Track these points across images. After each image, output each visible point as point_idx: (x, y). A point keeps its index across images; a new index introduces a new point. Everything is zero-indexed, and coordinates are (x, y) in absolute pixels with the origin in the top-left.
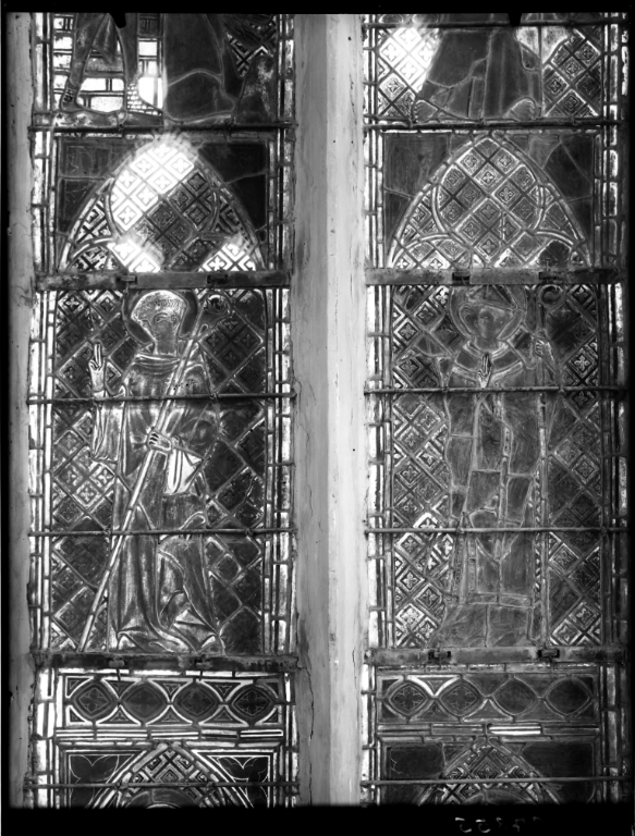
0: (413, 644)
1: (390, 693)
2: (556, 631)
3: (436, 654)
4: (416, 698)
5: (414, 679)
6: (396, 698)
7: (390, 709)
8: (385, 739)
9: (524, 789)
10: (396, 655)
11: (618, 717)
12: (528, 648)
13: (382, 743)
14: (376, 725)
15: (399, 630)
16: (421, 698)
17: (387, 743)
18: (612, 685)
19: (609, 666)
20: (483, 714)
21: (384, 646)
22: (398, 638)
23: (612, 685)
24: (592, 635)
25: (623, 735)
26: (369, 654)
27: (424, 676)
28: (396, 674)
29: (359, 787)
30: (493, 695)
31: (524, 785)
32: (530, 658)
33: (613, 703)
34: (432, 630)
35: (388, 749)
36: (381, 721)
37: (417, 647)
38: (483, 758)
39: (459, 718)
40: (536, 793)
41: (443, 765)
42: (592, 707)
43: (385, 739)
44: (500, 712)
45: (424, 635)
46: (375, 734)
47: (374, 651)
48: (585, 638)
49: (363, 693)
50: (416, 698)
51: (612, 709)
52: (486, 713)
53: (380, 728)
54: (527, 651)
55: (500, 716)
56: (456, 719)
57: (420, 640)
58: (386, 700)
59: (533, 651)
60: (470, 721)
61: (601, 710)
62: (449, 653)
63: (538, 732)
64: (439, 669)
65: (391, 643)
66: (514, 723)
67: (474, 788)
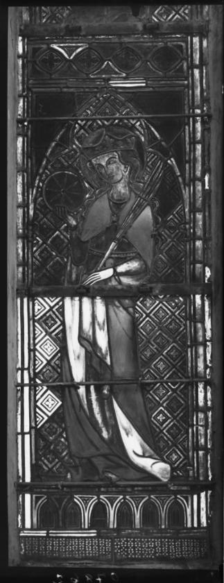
0: (54, 22)
1: (38, 57)
2: (156, 12)
3: (70, 27)
4: (57, 61)
5: (55, 47)
6: (42, 61)
7: (38, 68)
8: (34, 90)
9: (133, 125)
10: (42, 29)
11: (201, 73)
12: (136, 23)
13: (32, 92)
14: (28, 80)
15: (44, 12)
16: (60, 61)
17: (36, 93)
18: (196, 49)
19: (195, 36)
20: (104, 71)
21: (33, 23)
22: (44, 17)
23: (196, 49)
24: (183, 14)
25: (204, 85)
26: (22, 28)
27: (62, 45)
28: (43, 44)
29: (15, 122)
30: (111, 58)
31: (133, 122)
32: (138, 30)
33: (198, 63)
34: (67, 12)
35: (36, 97)
36: (31, 77)
37: (57, 23)
38: (104, 103)
39: (87, 75)
40: (142, 128)
41: (76, 108)
42: (182, 66)
43: (34, 90)
44: (117, 70)
45: (62, 16)
46: (27, 87)
47: (26, 26)
48: (177, 16)
49: (19, 57)
50: (57, 61)
51: (197, 67)
52: (104, 71)
53: (31, 82)
54: (135, 25)
55: (116, 73)
56: (85, 76)
57: (59, 19)
58: (35, 62)
59: (140, 26)
60: (95, 77)
61: (188, 68)
62: (80, 27)
63: (144, 85)
64: (73, 39)
65: (38, 21)
66: (125, 78)
67: (97, 124)
